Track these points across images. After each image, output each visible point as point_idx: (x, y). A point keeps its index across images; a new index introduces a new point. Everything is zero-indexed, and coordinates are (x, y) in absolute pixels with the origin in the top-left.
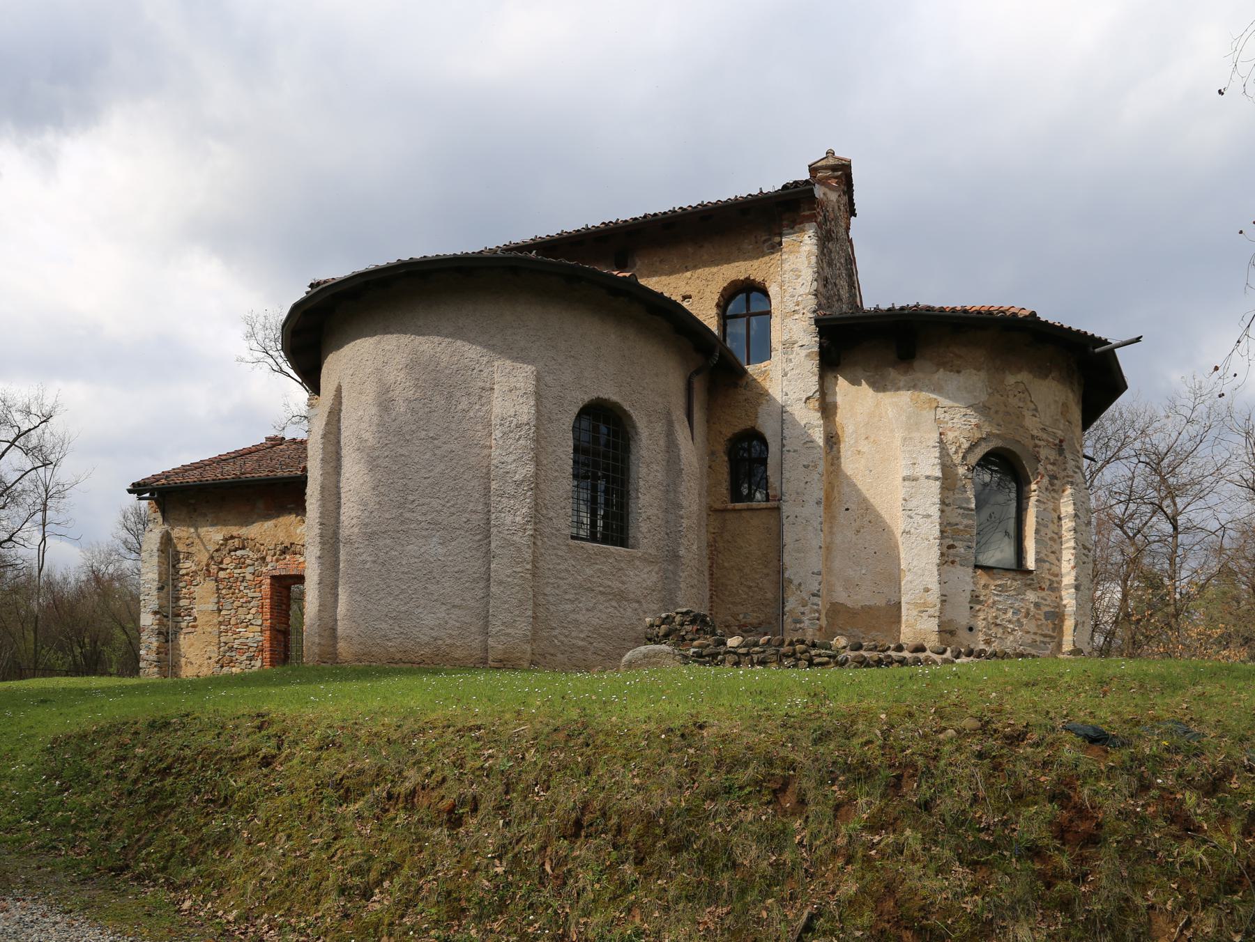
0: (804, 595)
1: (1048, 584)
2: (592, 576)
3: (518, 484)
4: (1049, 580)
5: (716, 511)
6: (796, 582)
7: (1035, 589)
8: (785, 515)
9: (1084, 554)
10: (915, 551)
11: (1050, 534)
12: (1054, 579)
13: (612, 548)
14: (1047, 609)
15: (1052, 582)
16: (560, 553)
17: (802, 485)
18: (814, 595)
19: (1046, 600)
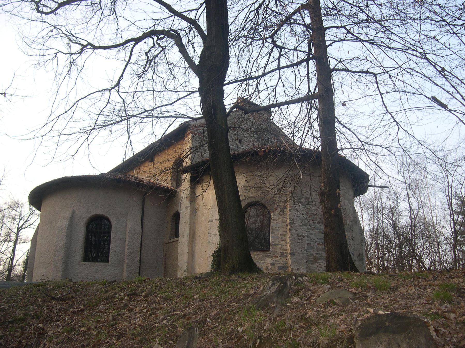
0: (182, 272)
1: (280, 254)
2: (88, 274)
3: (60, 247)
4: (280, 252)
5: (167, 243)
6: (180, 267)
7: (271, 257)
8: (179, 241)
9: (298, 239)
10: (211, 249)
11: (281, 232)
12: (284, 252)
13: (96, 263)
14: (279, 265)
15: (282, 253)
16: (76, 267)
17: (184, 229)
18: (185, 271)
19: (279, 261)
